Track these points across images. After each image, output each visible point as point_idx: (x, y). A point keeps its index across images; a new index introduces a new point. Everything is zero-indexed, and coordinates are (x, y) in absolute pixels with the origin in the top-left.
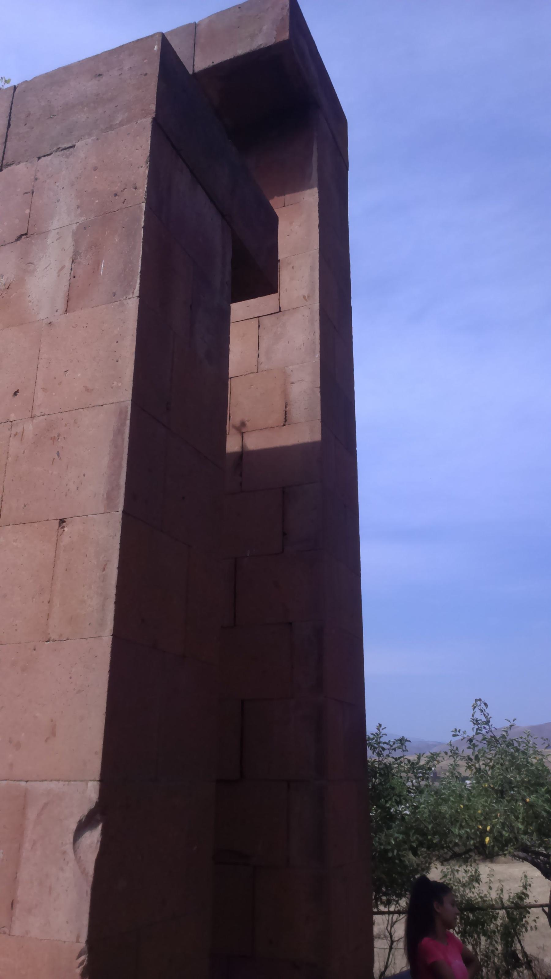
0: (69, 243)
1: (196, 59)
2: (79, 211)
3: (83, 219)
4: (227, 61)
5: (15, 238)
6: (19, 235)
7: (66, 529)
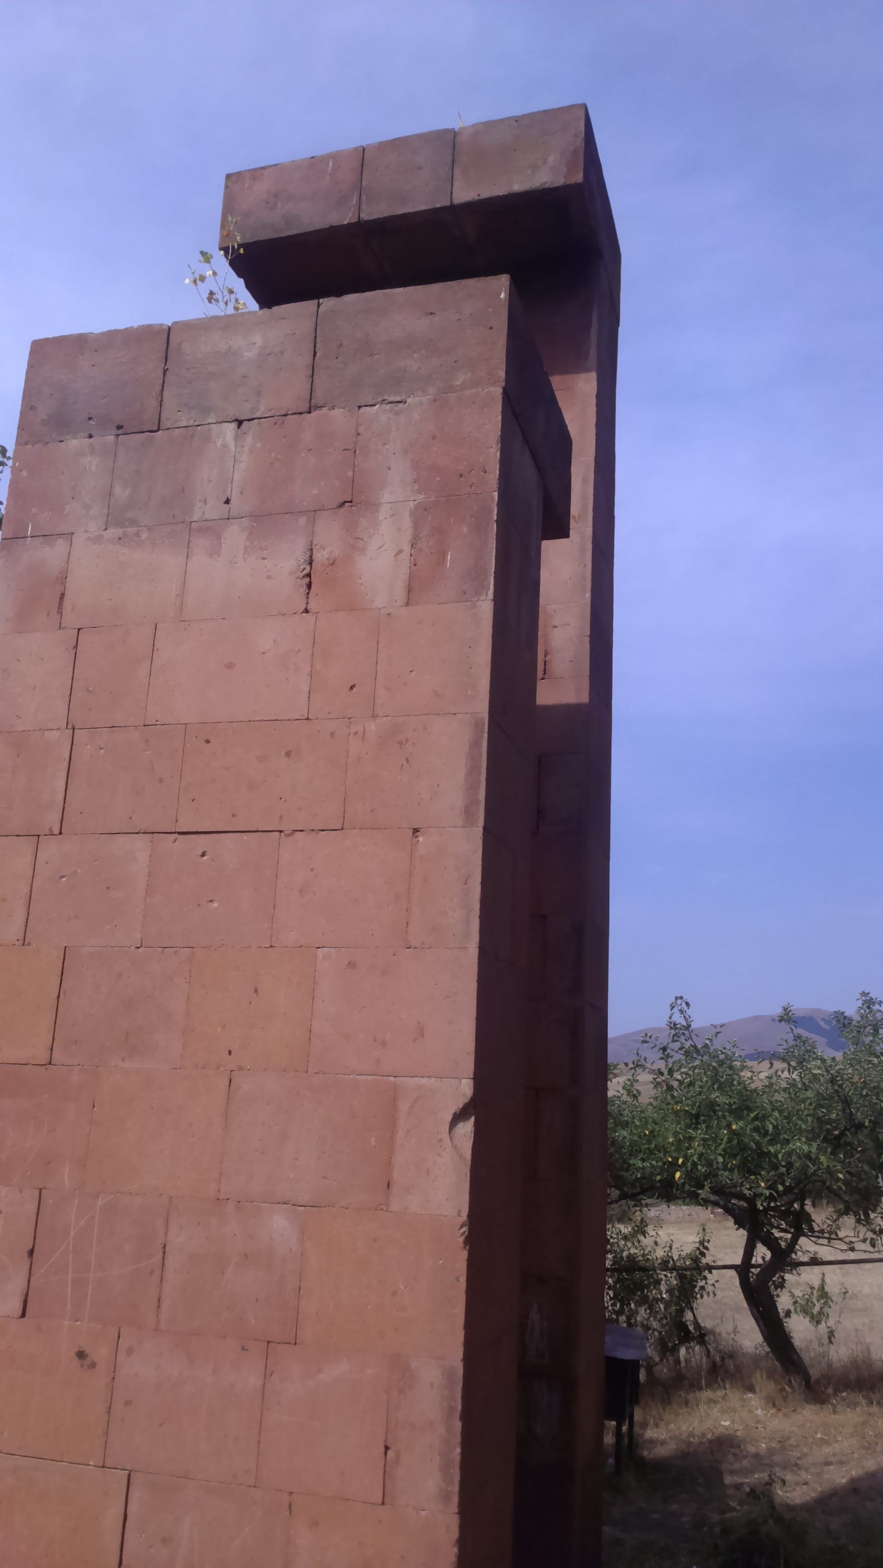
0: (407, 522)
1: (456, 184)
2: (416, 487)
3: (422, 496)
4: (498, 196)
5: (337, 504)
6: (342, 501)
7: (421, 839)
